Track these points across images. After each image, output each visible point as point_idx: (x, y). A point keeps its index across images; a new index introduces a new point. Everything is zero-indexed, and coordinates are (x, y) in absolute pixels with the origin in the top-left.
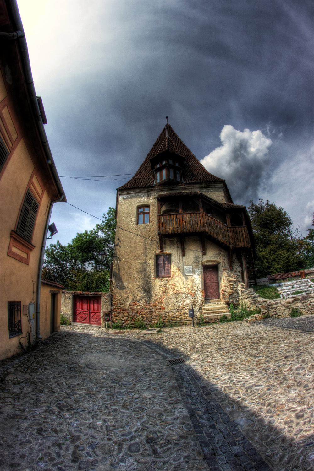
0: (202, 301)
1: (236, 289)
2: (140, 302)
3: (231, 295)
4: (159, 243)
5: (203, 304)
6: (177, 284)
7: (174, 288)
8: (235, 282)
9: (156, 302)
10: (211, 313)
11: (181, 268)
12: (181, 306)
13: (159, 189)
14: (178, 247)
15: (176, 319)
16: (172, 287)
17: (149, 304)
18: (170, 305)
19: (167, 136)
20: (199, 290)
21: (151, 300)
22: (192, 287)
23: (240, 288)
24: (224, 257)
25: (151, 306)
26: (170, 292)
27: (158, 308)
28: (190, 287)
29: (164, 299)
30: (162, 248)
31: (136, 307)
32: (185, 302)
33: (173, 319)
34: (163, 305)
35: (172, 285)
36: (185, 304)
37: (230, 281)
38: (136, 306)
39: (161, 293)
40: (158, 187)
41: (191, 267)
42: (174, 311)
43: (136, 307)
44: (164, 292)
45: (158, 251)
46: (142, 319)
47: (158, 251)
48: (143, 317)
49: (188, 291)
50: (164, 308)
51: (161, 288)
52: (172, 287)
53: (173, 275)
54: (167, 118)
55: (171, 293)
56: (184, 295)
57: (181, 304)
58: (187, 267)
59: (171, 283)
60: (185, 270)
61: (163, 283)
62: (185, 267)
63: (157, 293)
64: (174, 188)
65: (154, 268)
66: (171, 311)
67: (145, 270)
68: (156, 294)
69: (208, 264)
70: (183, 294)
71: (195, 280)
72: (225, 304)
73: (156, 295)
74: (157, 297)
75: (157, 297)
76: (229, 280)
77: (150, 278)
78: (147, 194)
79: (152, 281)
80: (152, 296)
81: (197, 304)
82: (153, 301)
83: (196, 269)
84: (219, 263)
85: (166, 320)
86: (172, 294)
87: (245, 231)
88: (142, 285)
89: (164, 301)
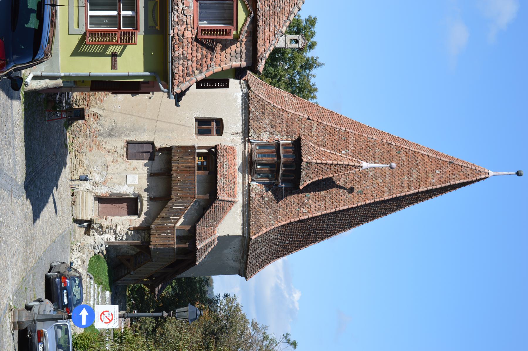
0: (97, 192)
1: (107, 232)
2: (97, 123)
3: (101, 227)
4: (168, 146)
5: (93, 194)
6: (118, 166)
7: (113, 162)
8: (115, 232)
9: (98, 143)
10: (83, 199)
11: (135, 171)
12: (93, 169)
13: (245, 149)
14: (161, 169)
15: (78, 164)
16: (115, 161)
17: (96, 134)
18: (94, 158)
19: (365, 165)
20: (110, 191)
21: (100, 137)
22: (114, 183)
23: (106, 236)
24: (146, 222)
25: (93, 136)
26: (109, 158)
27: (91, 144)
28: (113, 180)
29: (101, 152)
30: (161, 149)
31: (92, 119)
32: (96, 175)
33: (78, 160)
34: (94, 150)
35: (117, 160)
36: (94, 174)
37: (116, 226)
38: (94, 120)
39: (108, 148)
40: (249, 147)
41: (136, 182)
42: (87, 161)
43: (92, 119)
44: (109, 152)
45: (158, 145)
46: (79, 126)
47: (158, 145)
48: (81, 127)
49: (109, 177)
50: (90, 151)
51: (113, 148)
52: (115, 161)
53: (128, 162)
54: (518, 174)
55: (107, 159)
56: (105, 173)
57: (95, 169)
58: (137, 178)
59: (120, 159)
60: (133, 175)
61: (119, 150)
62: (137, 176)
63: (109, 143)
64: (245, 168)
65: (138, 140)
66: (88, 159)
67: (135, 130)
68: (107, 143)
69: (139, 203)
70: (106, 173)
71: (121, 186)
72: (91, 219)
73: (106, 143)
74: (103, 143)
75: (103, 143)
76: (118, 225)
77: (126, 135)
78: (241, 131)
79: (123, 137)
80: (105, 137)
81: (93, 187)
82: (99, 138)
83: (133, 188)
84: (139, 217)
85: (77, 153)
86: (106, 160)
87: (169, 244)
88: (118, 127)
89: (99, 151)
